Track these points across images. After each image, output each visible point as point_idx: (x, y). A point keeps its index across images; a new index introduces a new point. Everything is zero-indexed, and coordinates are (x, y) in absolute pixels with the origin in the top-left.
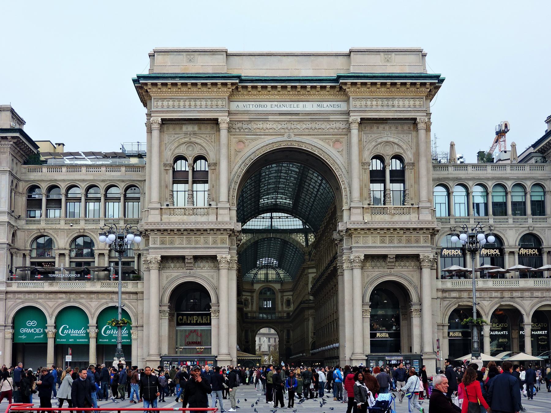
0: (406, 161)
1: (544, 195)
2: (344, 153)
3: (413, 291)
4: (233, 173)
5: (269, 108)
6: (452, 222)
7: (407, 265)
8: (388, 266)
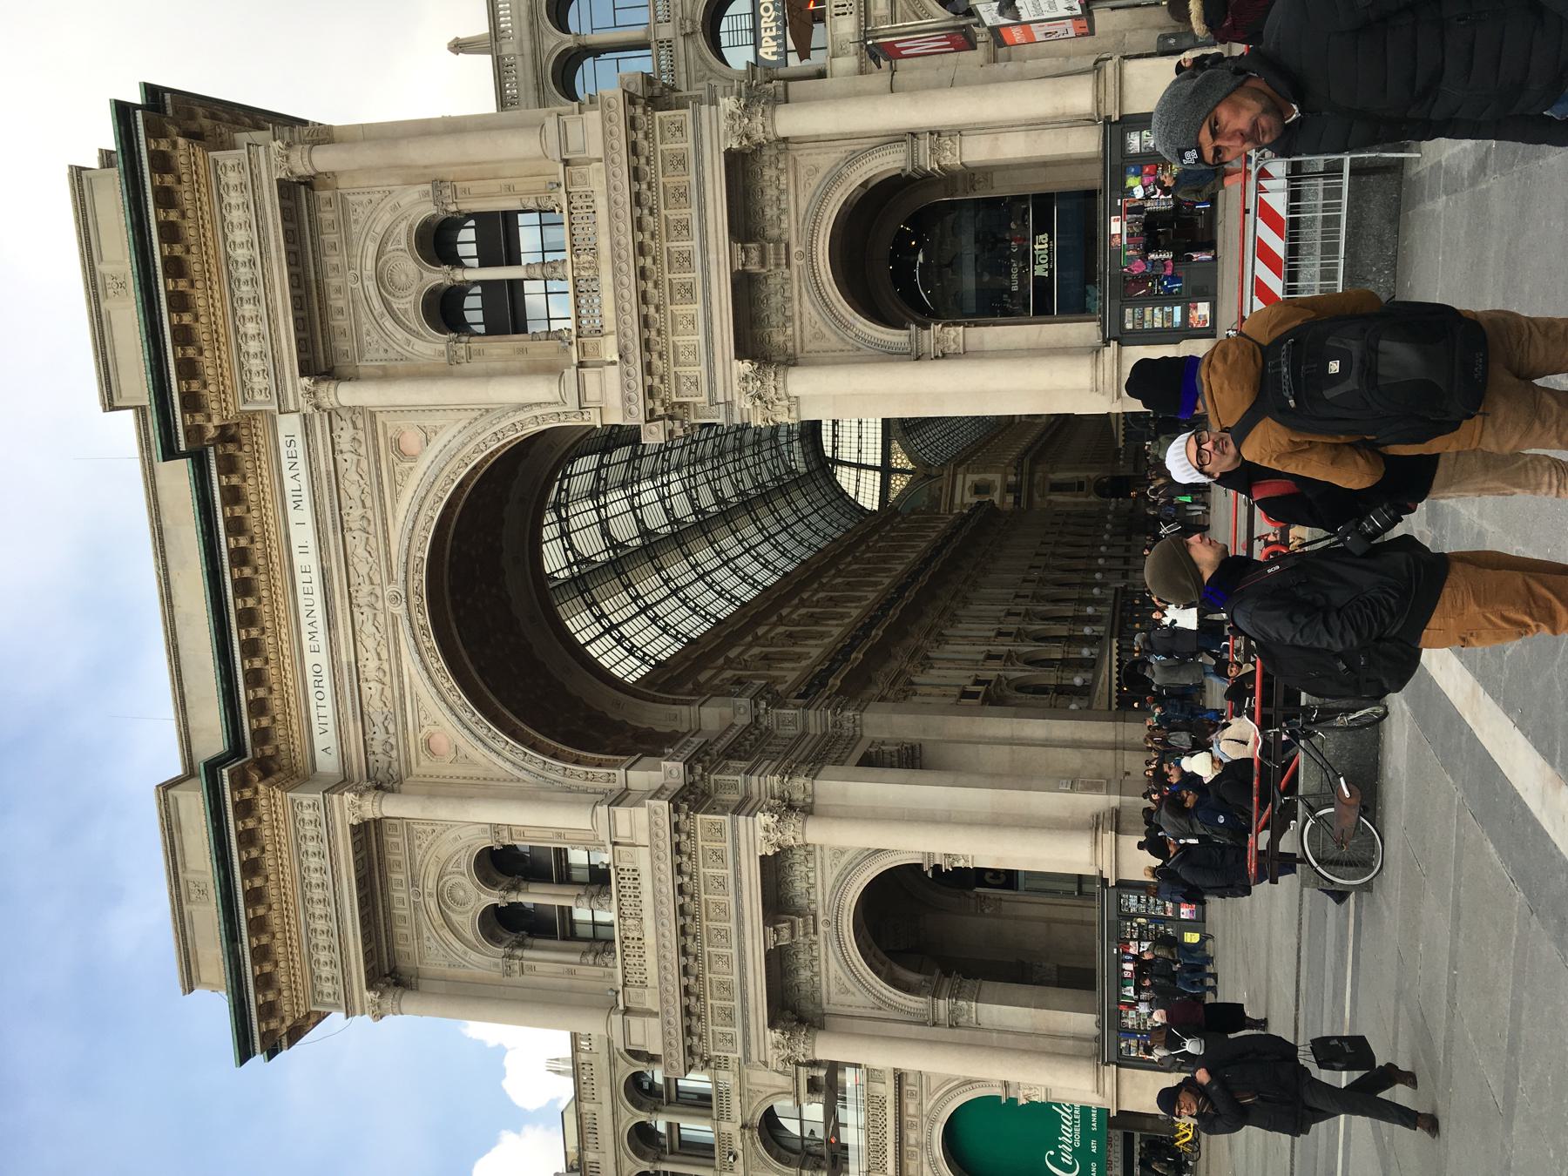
2: (428, 422)
3: (865, 168)
4: (516, 772)
5: (323, 658)
6: (666, 32)
7: (775, 193)
8: (778, 265)
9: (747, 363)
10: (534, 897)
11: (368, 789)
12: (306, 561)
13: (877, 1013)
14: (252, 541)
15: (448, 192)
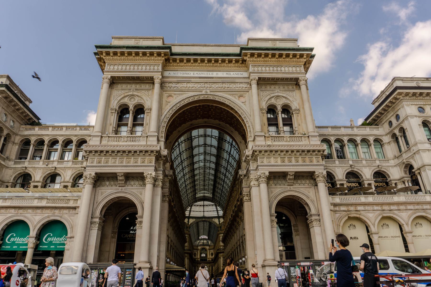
0: (293, 108)
1: (382, 147)
5: (192, 75)
8: (288, 183)
9: (268, 174)
10: (130, 117)
11: (161, 81)
12: (215, 74)
13: (95, 202)
14: (220, 64)
15: (298, 112)
